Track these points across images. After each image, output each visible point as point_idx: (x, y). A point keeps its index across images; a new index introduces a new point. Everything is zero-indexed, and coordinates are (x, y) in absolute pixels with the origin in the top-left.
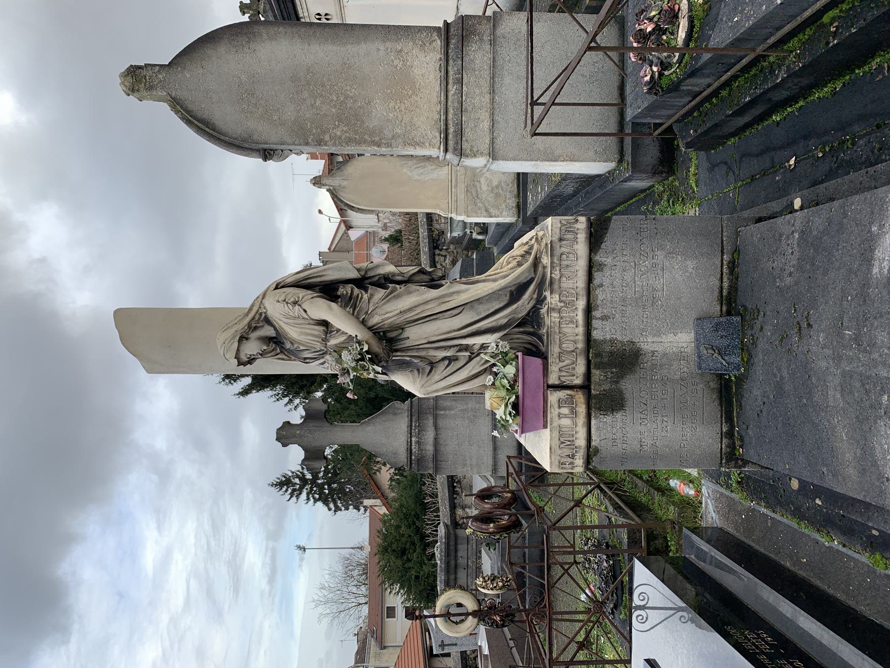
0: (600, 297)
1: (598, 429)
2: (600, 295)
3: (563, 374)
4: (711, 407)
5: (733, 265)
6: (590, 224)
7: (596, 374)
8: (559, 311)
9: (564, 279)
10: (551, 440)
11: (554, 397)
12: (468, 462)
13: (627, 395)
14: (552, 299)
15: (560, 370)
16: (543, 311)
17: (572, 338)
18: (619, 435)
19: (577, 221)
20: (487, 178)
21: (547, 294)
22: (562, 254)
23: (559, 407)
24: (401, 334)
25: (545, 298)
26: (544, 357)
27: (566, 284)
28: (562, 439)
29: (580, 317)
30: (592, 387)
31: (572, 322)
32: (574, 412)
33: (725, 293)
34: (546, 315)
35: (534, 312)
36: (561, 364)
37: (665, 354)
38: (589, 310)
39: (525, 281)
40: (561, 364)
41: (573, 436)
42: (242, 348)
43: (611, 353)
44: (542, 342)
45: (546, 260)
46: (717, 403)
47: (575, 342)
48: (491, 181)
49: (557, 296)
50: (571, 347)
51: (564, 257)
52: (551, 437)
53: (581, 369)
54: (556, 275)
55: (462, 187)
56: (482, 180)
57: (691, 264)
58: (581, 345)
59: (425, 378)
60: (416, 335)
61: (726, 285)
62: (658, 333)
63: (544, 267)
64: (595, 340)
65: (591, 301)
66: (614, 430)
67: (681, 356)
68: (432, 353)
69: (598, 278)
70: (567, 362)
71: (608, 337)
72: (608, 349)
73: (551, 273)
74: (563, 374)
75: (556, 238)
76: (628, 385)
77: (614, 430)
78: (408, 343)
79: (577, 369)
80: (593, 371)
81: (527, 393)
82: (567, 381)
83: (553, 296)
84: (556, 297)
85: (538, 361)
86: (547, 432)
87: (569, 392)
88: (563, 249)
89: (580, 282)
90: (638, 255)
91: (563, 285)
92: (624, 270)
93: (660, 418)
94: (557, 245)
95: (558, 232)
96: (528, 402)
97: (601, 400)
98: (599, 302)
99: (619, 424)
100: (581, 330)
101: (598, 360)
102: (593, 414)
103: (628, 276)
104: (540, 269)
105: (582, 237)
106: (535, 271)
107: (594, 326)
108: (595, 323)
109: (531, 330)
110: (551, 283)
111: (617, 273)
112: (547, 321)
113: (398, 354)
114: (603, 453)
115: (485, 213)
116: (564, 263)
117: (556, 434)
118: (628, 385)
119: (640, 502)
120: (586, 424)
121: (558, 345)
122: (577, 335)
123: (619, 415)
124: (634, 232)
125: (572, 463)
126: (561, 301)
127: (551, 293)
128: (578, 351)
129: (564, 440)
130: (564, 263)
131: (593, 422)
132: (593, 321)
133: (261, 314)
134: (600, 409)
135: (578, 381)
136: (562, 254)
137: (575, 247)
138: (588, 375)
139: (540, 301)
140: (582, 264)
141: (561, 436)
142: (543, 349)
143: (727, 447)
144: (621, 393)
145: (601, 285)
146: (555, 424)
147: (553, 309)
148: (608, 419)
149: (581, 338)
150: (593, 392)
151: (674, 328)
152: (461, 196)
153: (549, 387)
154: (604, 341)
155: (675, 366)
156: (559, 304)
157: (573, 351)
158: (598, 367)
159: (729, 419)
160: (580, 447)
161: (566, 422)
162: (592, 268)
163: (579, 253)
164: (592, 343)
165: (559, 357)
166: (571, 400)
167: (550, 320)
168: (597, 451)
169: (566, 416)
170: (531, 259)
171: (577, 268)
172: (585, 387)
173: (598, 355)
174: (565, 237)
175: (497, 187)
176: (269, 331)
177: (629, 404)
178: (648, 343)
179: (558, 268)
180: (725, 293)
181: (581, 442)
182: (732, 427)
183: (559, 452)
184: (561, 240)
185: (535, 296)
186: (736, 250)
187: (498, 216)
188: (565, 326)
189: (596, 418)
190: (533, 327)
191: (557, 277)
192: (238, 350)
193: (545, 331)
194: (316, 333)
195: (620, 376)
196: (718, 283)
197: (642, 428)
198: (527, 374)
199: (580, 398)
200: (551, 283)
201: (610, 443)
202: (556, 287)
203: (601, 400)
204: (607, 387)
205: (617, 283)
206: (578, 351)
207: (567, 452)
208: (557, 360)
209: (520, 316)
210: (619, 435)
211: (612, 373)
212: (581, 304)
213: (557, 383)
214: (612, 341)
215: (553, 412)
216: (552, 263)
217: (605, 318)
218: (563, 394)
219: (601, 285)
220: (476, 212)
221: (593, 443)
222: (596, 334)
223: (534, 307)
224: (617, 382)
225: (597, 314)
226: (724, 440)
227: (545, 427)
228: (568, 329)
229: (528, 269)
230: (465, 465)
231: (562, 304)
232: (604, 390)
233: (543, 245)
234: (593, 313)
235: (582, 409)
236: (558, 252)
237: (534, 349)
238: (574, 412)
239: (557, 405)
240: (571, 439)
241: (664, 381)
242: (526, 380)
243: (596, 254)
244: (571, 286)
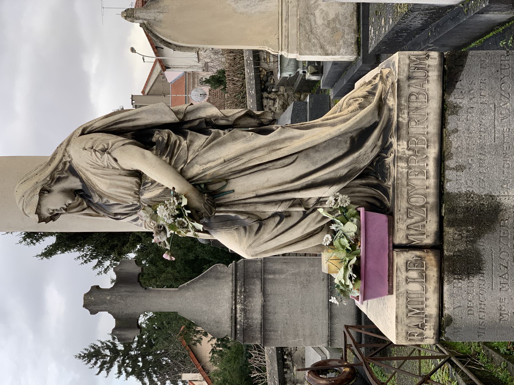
0: (454, 145)
1: (451, 295)
2: (455, 142)
3: (412, 232)
6: (443, 60)
7: (450, 232)
8: (407, 160)
9: (413, 123)
10: (397, 308)
11: (401, 259)
12: (300, 333)
13: (486, 257)
14: (399, 146)
15: (408, 228)
16: (389, 160)
17: (422, 191)
18: (476, 302)
19: (428, 56)
20: (322, 11)
21: (393, 140)
22: (410, 95)
23: (407, 270)
24: (225, 186)
25: (391, 145)
27: (415, 129)
28: (410, 307)
29: (431, 167)
30: (445, 247)
31: (422, 173)
32: (424, 277)
34: (391, 165)
35: (378, 162)
36: (409, 221)
38: (441, 160)
39: (369, 125)
40: (409, 221)
41: (422, 303)
42: (44, 202)
43: (467, 209)
44: (387, 195)
45: (392, 102)
47: (425, 196)
48: (327, 14)
49: (405, 143)
50: (421, 202)
51: (413, 98)
52: (398, 305)
53: (432, 226)
54: (404, 118)
55: (293, 21)
56: (317, 13)
58: (432, 200)
59: (253, 238)
60: (242, 187)
63: (390, 110)
64: (448, 193)
65: (445, 148)
66: (470, 297)
68: (261, 208)
69: (452, 122)
70: (416, 218)
71: (464, 190)
72: (463, 203)
73: (398, 117)
74: (412, 232)
75: (403, 76)
76: (486, 246)
77: (470, 297)
78: (233, 197)
79: (427, 227)
80: (446, 229)
81: (370, 254)
82: (416, 240)
83: (400, 143)
84: (404, 144)
85: (383, 218)
86: (393, 298)
87: (418, 253)
88: (412, 89)
89: (432, 127)
90: (498, 96)
91: (412, 130)
92: (482, 113)
94: (405, 85)
95: (406, 69)
96: (371, 265)
97: (456, 263)
98: (453, 150)
99: (476, 290)
100: (432, 182)
101: (452, 216)
102: (446, 279)
103: (487, 120)
104: (385, 112)
105: (434, 75)
106: (380, 114)
107: (447, 177)
108: (449, 174)
109: (375, 182)
110: (398, 128)
111: (474, 116)
112: (394, 172)
113: (222, 209)
114: (457, 322)
115: (320, 51)
116: (414, 105)
117: (403, 301)
118: (486, 246)
119: (497, 378)
120: (437, 290)
121: (405, 200)
122: (427, 188)
123: (475, 280)
124: (493, 70)
125: (421, 334)
126: (409, 149)
127: (398, 139)
128: (429, 206)
129: (413, 308)
130: (414, 105)
131: (446, 287)
132: (447, 172)
133: (65, 164)
134: (454, 272)
135: (429, 241)
136: (410, 95)
137: (426, 86)
138: (440, 234)
139: (386, 148)
141: (408, 303)
142: (389, 204)
145: (456, 131)
146: (402, 290)
147: (400, 158)
148: (463, 284)
149: (432, 191)
150: (446, 253)
152: (293, 31)
153: (396, 247)
154: (459, 195)
156: (407, 152)
157: (423, 206)
158: (451, 224)
160: (430, 316)
161: (414, 287)
162: (445, 110)
163: (430, 93)
164: (445, 197)
165: (407, 213)
166: (420, 263)
167: (397, 170)
168: (450, 320)
169: (414, 281)
171: (428, 110)
172: (437, 247)
173: (452, 210)
174: (414, 75)
175: (334, 20)
176: (74, 183)
177: (487, 266)
179: (406, 111)
181: (432, 310)
183: (407, 321)
184: (409, 78)
185: (380, 143)
187: (335, 54)
188: (413, 176)
189: (449, 282)
190: (377, 179)
191: (405, 122)
192: (39, 204)
193: (390, 183)
194: (128, 185)
195: (478, 235)
197: (503, 295)
198: (371, 233)
199: (431, 259)
200: (398, 128)
201: (465, 312)
202: (403, 132)
203: (456, 263)
204: (462, 247)
205: (474, 127)
206: (429, 206)
207: (416, 321)
208: (405, 217)
209: (362, 165)
210: (476, 302)
211: (468, 231)
212: (433, 152)
213: (404, 242)
214: (468, 195)
215: (400, 276)
216: (399, 105)
217: (460, 168)
218: (411, 255)
219: (456, 131)
220: (310, 50)
221: (446, 312)
222: (450, 187)
223: (378, 155)
224: (474, 242)
225: (450, 163)
227: (390, 292)
228: (417, 181)
229: (372, 112)
230: (297, 335)
231: (411, 153)
232: (459, 251)
233: (389, 84)
234: (447, 163)
235: (433, 273)
236: (406, 92)
237: (378, 204)
238: (424, 277)
239: (403, 268)
240: (420, 306)
242: (370, 239)
243: (450, 94)
244: (421, 131)
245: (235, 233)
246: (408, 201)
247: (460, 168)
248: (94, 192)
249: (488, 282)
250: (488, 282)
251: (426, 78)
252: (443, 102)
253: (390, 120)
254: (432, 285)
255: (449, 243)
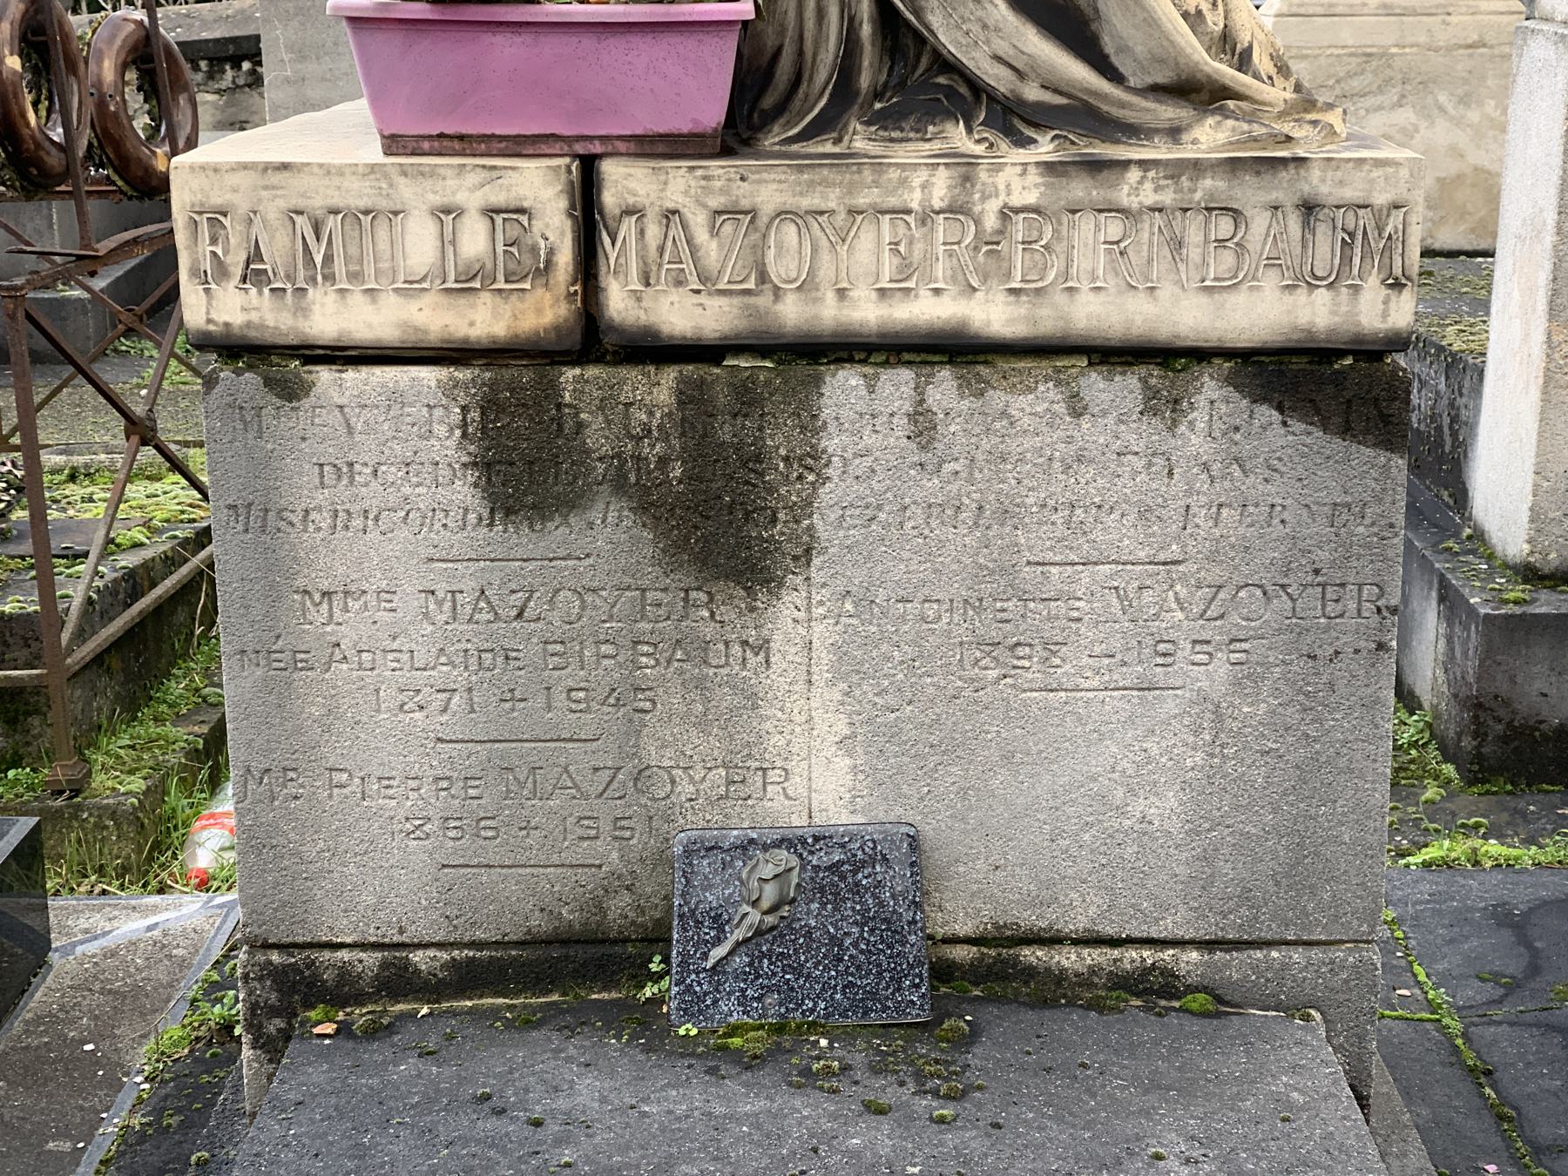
0: (1021, 404)
1: (396, 398)
2: (1031, 403)
3: (653, 231)
4: (521, 894)
5: (1156, 989)
6: (1372, 352)
7: (660, 389)
8: (956, 209)
9: (1114, 228)
10: (327, 170)
11: (540, 185)
12: (311, 67)
13: (558, 534)
14: (1016, 174)
15: (670, 214)
16: (958, 136)
17: (826, 271)
18: (371, 494)
19: (1397, 286)
21: (1045, 148)
22: (1235, 214)
23: (491, 212)
25: (1023, 142)
26: (739, 133)
27: (1089, 238)
28: (332, 223)
29: (927, 310)
30: (592, 371)
31: (906, 269)
33: (1032, 955)
34: (936, 146)
35: (950, 92)
36: (698, 221)
37: (753, 700)
39: (1109, 47)
40: (698, 221)
41: (354, 276)
43: (756, 459)
44: (802, 137)
45: (1210, 136)
46: (539, 923)
47: (807, 286)
49: (1031, 198)
51: (1225, 226)
52: (340, 171)
53: (681, 314)
54: (1135, 190)
56: (1405, 116)
57: (1164, 808)
58: (792, 314)
61: (1068, 959)
62: (848, 668)
63: (1174, 133)
64: (818, 381)
65: (1003, 364)
66: (391, 473)
67: (744, 768)
70: (711, 250)
71: (832, 443)
72: (778, 442)
73: (1144, 164)
74: (653, 231)
75: (1318, 183)
76: (606, 535)
77: (391, 473)
79: (675, 295)
80: (669, 376)
81: (552, 45)
83: (1034, 177)
84: (1027, 190)
85: (711, 112)
86: (373, 152)
87: (565, 258)
88: (1259, 223)
90: (1216, 574)
91: (1086, 222)
92: (1145, 513)
93: (459, 678)
94: (1283, 189)
95: (1350, 194)
97: (533, 412)
98: (997, 398)
99: (423, 497)
100: (867, 313)
102: (464, 374)
103: (1120, 533)
104: (1168, 112)
105: (1316, 313)
106: (1158, 91)
107: (886, 375)
108: (898, 383)
109: (865, 81)
110: (1095, 166)
111: (1135, 480)
112: (910, 153)
114: (284, 422)
116: (1193, 231)
117: (357, 194)
118: (606, 535)
119: (168, 675)
120: (412, 339)
121: (790, 201)
122: (841, 293)
123: (464, 493)
124: (1323, 556)
125: (222, 271)
126: (1007, 213)
127: (1049, 168)
128: (764, 301)
129: (329, 238)
130: (1193, 231)
132: (906, 374)
134: (490, 405)
136: (1235, 214)
137: (1270, 281)
138: (650, 350)
139: (1010, 118)
140: (1183, 314)
142: (770, 141)
143: (344, 971)
144: (570, 503)
145: (1077, 408)
146: (406, 191)
147: (967, 179)
148: (446, 446)
149: (827, 314)
150: (571, 373)
151: (873, 738)
153: (589, 170)
154: (811, 425)
155: (700, 744)
156: (993, 206)
157: (763, 277)
158: (689, 396)
159: (470, 976)
160: (302, 310)
161: (419, 245)
162: (1163, 361)
163: (1240, 299)
164: (802, 369)
165: (732, 212)
166: (521, 266)
167: (918, 167)
168: (291, 392)
169: (448, 242)
170: (1224, 71)
171: (1166, 291)
172: (592, 339)
173: (747, 398)
174: (1322, 230)
177: (520, 539)
178: (801, 622)
179: (1167, 198)
180: (1032, 955)
181: (329, 317)
182: (431, 989)
183: (273, 209)
184: (1309, 208)
185: (1032, 93)
186: (1221, 1003)
189: (449, 389)
190: (878, 95)
193: (859, 144)
195: (649, 502)
196: (1078, 923)
197: (409, 602)
198: (646, 50)
199: (542, 311)
200: (1095, 166)
201: (330, 452)
202: (1080, 188)
203: (533, 412)
204: (598, 438)
205: (1091, 483)
206: (764, 301)
207: (277, 249)
208: (715, 202)
209: (936, 20)
211: (663, 461)
212: (993, 315)
213: (610, 199)
214: (812, 461)
215: (467, 183)
216: (1196, 167)
217: (923, 425)
218: (555, 227)
219: (1077, 408)
222: (844, 386)
223: (977, 88)
224: (619, 485)
225: (944, 388)
226: (371, 959)
227: (394, 144)
228: (869, 250)
229: (1166, 53)
230: (301, 55)
231: (991, 222)
232: (580, 426)
233: (1286, 128)
234: (945, 373)
235: (484, 320)
236: (1251, 194)
237: (768, 102)
238: (470, 282)
239: (498, 198)
240: (339, 267)
241: (631, 698)
242: (615, 46)
243: (1231, 380)
244: (1082, 263)
246: (782, 214)
249: (457, 542)
250: (457, 542)
251: (1311, 282)
252: (1200, 355)
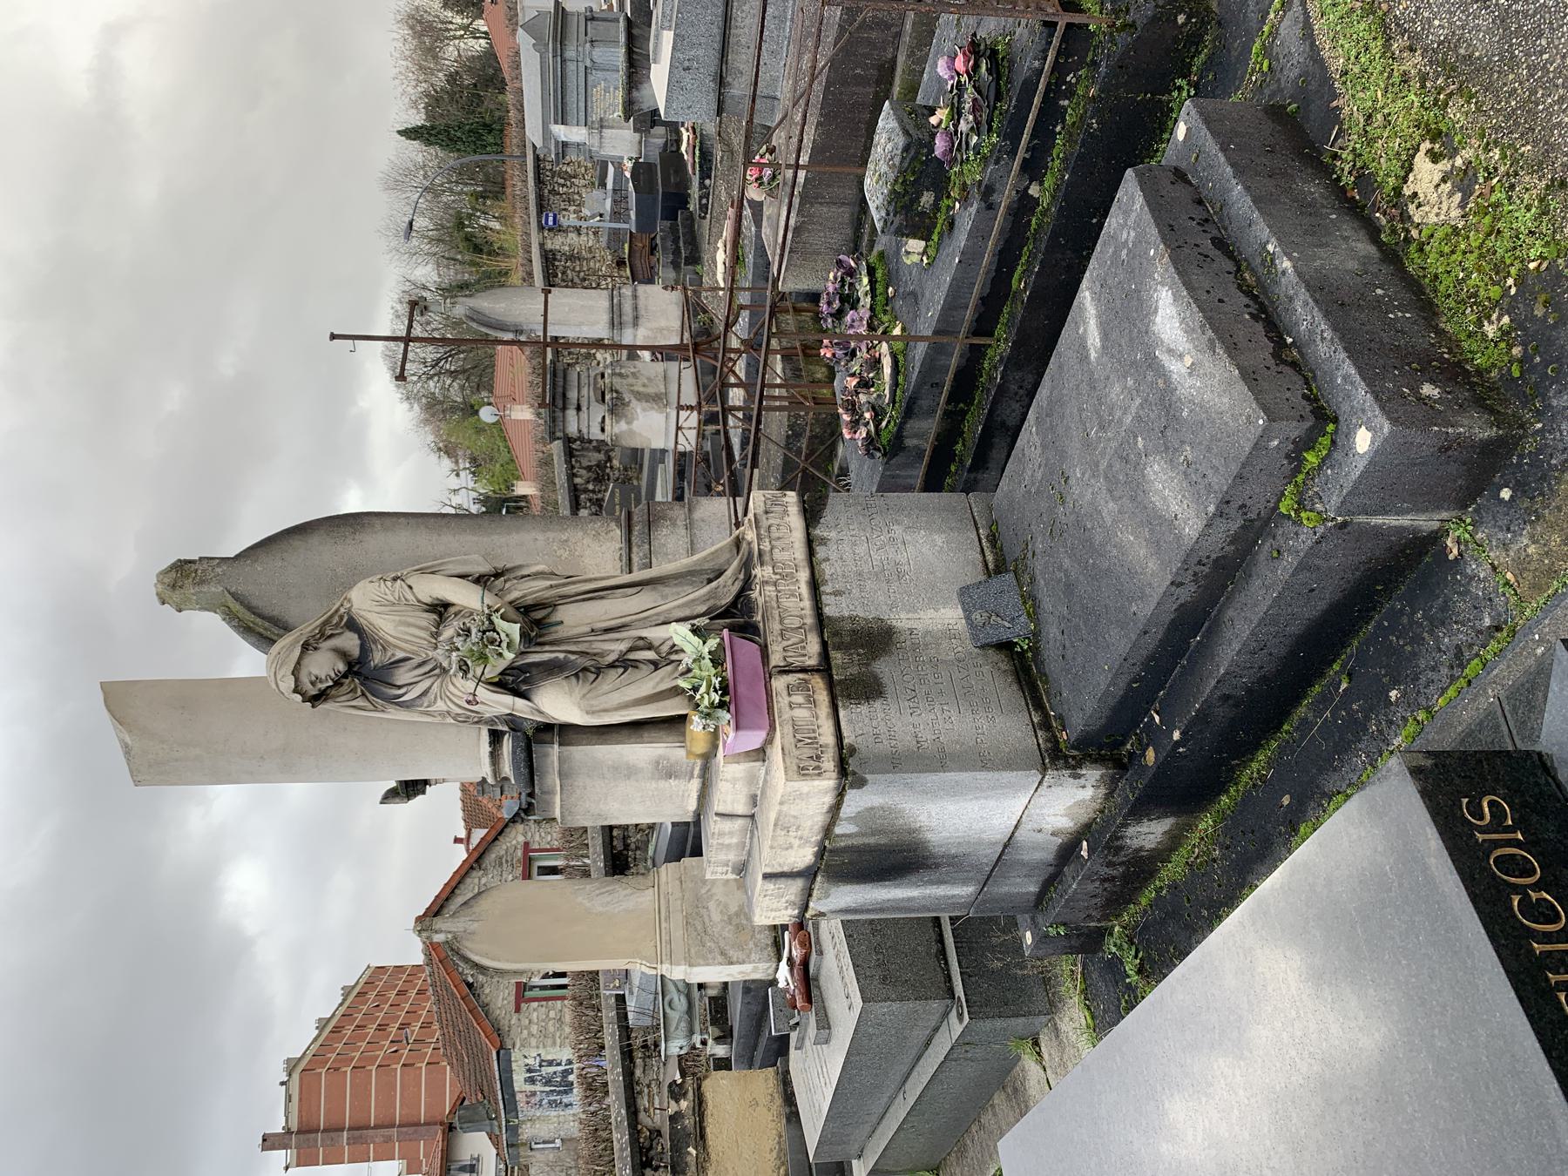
1: (850, 721)
2: (827, 570)
5: (993, 539)
7: (837, 657)
8: (775, 584)
11: (779, 683)
13: (885, 680)
20: (719, 903)
24: (548, 615)
29: (804, 590)
32: (811, 701)
33: (991, 566)
36: (785, 643)
37: (927, 632)
38: (815, 585)
40: (785, 643)
42: (305, 662)
46: (1015, 687)
48: (726, 906)
50: (796, 623)
53: (814, 646)
54: (766, 546)
55: (677, 919)
56: (712, 905)
57: (939, 539)
58: (810, 621)
59: (587, 687)
60: (574, 619)
61: (990, 558)
62: (913, 609)
66: (874, 723)
67: (950, 635)
68: (599, 646)
69: (821, 552)
72: (848, 627)
76: (883, 668)
77: (874, 723)
78: (561, 632)
81: (739, 678)
82: (797, 661)
84: (768, 570)
87: (801, 676)
89: (800, 552)
93: (937, 707)
96: (742, 689)
99: (881, 715)
100: (807, 603)
101: (837, 640)
103: (861, 550)
104: (744, 545)
110: (760, 555)
113: (547, 648)
115: (720, 958)
118: (883, 668)
123: (878, 704)
131: (842, 713)
133: (341, 618)
134: (849, 697)
135: (812, 662)
138: (825, 655)
139: (747, 584)
140: (798, 535)
141: (796, 731)
143: (1047, 741)
144: (876, 678)
146: (785, 716)
151: (933, 603)
152: (678, 934)
154: (843, 619)
155: (945, 644)
158: (838, 648)
159: (1039, 706)
160: (827, 746)
162: (810, 544)
166: (804, 687)
172: (824, 667)
173: (836, 634)
175: (737, 915)
176: (350, 642)
177: (889, 689)
178: (901, 620)
180: (991, 566)
181: (828, 737)
182: (1046, 716)
185: (742, 576)
186: (993, 523)
187: (743, 962)
188: (785, 601)
191: (768, 548)
192: (298, 663)
194: (424, 623)
196: (979, 557)
197: (915, 719)
198: (738, 655)
199: (818, 682)
202: (767, 558)
204: (854, 670)
205: (848, 556)
207: (808, 752)
210: (883, 729)
212: (804, 575)
214: (852, 619)
215: (781, 701)
216: (758, 535)
217: (837, 593)
218: (792, 679)
220: (705, 958)
221: (846, 741)
222: (827, 611)
224: (868, 665)
226: (1040, 733)
235: (823, 697)
236: (764, 523)
241: (935, 663)
245: (564, 683)
246: (781, 622)
247: (837, 593)
248: (375, 642)
249: (894, 707)
250: (894, 707)
251: (786, 512)
252: (808, 534)
253: (750, 553)
254: (824, 709)
255: (838, 666)
